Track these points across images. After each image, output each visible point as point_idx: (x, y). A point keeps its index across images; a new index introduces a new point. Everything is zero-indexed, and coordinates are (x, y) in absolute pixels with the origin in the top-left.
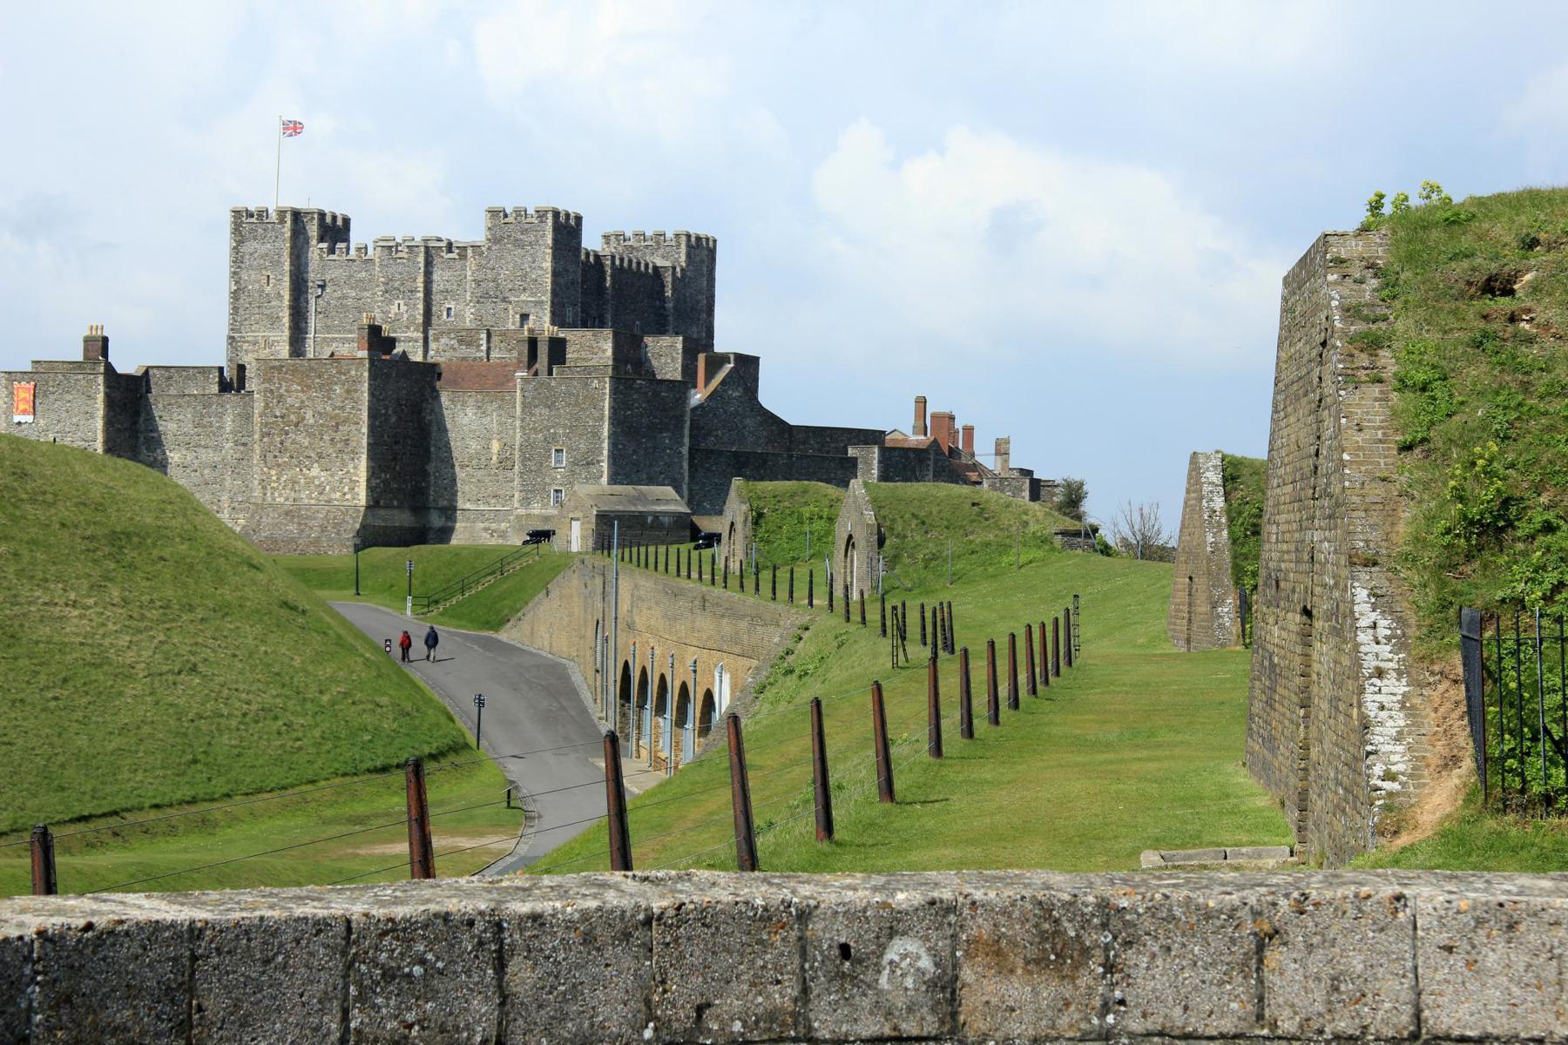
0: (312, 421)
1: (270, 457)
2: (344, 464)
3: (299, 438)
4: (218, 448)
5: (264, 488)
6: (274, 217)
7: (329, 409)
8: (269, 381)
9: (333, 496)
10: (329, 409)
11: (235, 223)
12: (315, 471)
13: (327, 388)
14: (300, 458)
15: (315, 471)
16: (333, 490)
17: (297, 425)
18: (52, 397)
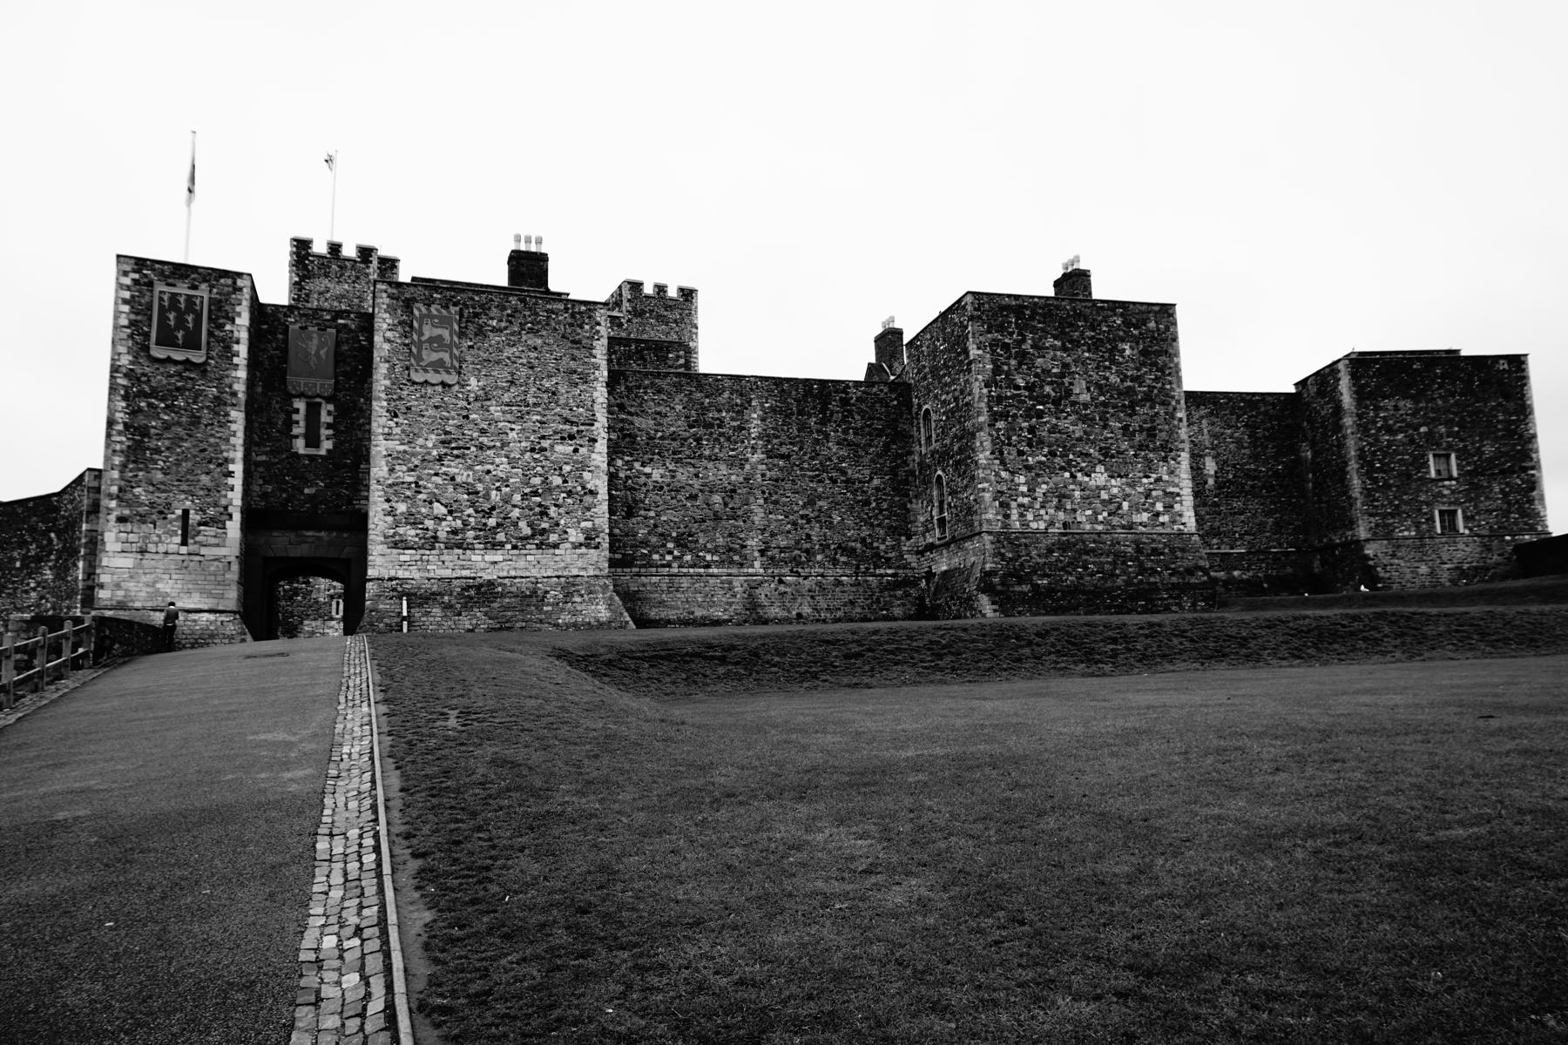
0: (1085, 397)
1: (1010, 454)
2: (1149, 468)
3: (1062, 424)
4: (738, 462)
5: (1005, 505)
6: (349, 251)
7: (1114, 379)
8: (1001, 329)
9: (1137, 518)
10: (1114, 379)
11: (297, 254)
12: (1100, 477)
13: (1106, 348)
14: (1065, 455)
15: (1100, 477)
16: (1136, 508)
17: (1056, 402)
18: (495, 339)
